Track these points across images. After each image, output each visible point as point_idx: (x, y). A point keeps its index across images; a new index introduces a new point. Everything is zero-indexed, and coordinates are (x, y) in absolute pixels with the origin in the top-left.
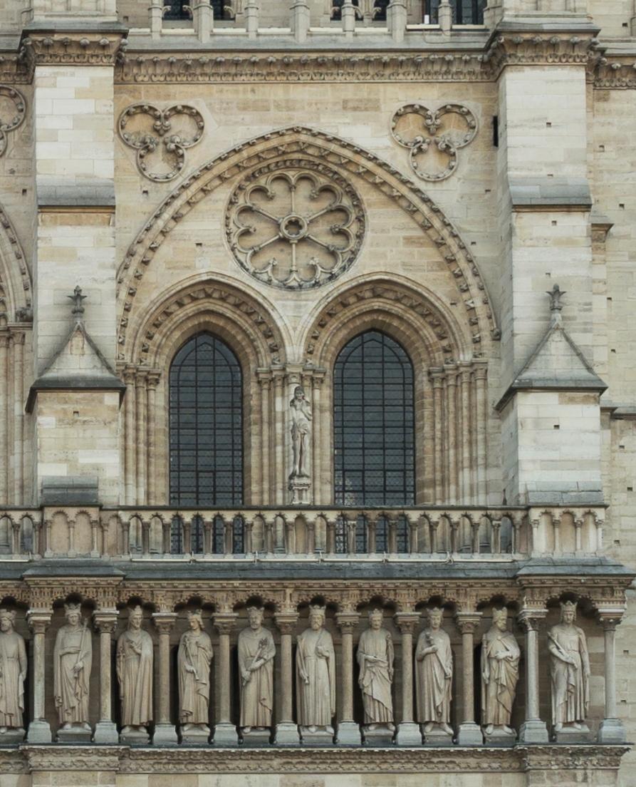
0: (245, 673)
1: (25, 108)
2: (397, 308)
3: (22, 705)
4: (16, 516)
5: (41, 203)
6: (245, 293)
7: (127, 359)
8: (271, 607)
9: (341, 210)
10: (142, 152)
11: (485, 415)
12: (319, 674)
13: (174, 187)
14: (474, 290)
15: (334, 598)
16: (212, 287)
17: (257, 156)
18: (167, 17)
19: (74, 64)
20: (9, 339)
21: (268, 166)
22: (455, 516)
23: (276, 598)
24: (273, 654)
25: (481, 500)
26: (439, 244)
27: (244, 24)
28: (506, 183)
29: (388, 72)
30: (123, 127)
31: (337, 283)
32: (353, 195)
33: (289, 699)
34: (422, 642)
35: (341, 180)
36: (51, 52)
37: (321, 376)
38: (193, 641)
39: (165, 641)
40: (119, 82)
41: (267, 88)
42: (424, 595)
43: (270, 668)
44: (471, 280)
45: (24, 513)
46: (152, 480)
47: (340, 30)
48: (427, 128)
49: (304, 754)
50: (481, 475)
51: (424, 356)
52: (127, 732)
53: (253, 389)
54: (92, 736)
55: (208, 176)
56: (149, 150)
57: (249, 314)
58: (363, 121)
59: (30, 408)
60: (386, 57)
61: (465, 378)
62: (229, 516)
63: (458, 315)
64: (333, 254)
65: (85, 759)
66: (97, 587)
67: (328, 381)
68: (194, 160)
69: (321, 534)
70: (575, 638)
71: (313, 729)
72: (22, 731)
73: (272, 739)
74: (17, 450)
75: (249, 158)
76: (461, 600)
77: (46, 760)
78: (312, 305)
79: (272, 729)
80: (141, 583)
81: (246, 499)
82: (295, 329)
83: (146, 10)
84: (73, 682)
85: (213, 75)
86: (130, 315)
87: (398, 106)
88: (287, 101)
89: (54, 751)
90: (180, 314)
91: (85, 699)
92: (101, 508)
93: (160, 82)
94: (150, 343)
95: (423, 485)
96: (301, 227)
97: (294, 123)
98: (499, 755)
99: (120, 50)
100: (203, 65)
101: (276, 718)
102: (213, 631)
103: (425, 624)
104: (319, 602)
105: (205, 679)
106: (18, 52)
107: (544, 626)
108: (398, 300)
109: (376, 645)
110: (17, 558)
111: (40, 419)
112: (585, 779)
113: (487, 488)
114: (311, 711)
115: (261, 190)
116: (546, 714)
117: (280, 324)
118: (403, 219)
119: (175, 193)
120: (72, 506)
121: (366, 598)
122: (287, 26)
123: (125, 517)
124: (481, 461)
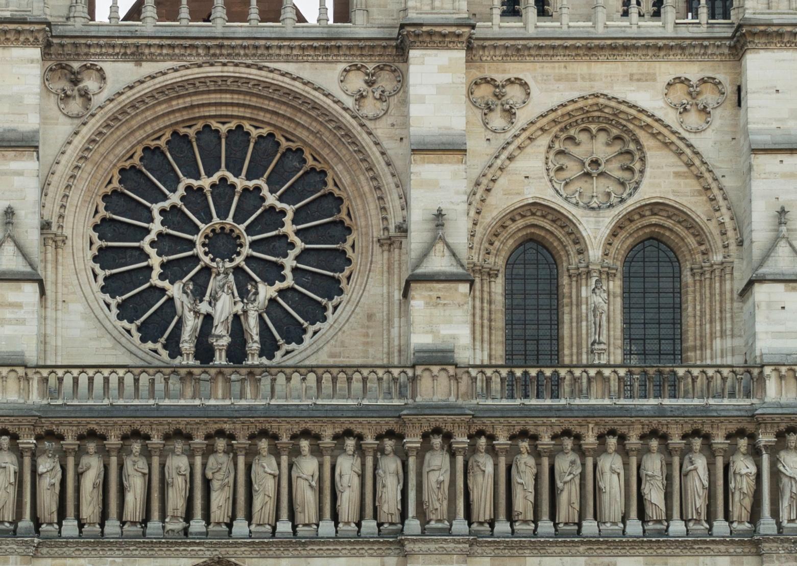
0: (559, 484)
1: (402, 79)
2: (669, 223)
3: (399, 507)
4: (396, 372)
5: (413, 147)
6: (559, 212)
7: (475, 259)
8: (578, 437)
9: (629, 152)
10: (486, 111)
11: (732, 299)
12: (613, 485)
13: (508, 136)
15: (623, 431)
16: (536, 208)
17: (568, 114)
18: (504, 14)
19: (437, 48)
20: (390, 245)
21: (576, 121)
22: (710, 372)
23: (582, 431)
24: (579, 470)
25: (729, 360)
26: (699, 177)
27: (558, 19)
28: (746, 133)
29: (662, 53)
30: (472, 93)
31: (625, 205)
32: (637, 141)
33: (591, 503)
34: (686, 462)
35: (628, 131)
36: (420, 39)
37: (614, 271)
38: (523, 462)
39: (502, 461)
40: (469, 61)
41: (576, 65)
42: (688, 429)
43: (577, 480)
44: (721, 202)
45: (401, 369)
46: (493, 346)
47: (627, 24)
48: (690, 94)
49: (602, 543)
50: (729, 343)
51: (688, 257)
52: (475, 526)
53: (565, 280)
54: (450, 529)
55: (533, 128)
56: (491, 110)
57: (562, 227)
58: (644, 89)
59: (406, 294)
60: (661, 43)
61: (717, 273)
62: (548, 372)
63: (712, 228)
64: (622, 184)
65: (445, 546)
66: (453, 422)
67: (619, 275)
68: (523, 117)
69: (614, 385)
71: (608, 525)
72: (400, 526)
73: (579, 531)
74: (396, 324)
75: (563, 116)
76: (715, 432)
77: (417, 547)
78: (608, 220)
79: (579, 525)
80: (485, 420)
81: (560, 359)
82: (595, 238)
83: (488, 10)
84: (436, 490)
85: (537, 55)
86: (477, 228)
87: (669, 78)
88: (590, 74)
89: (423, 540)
90: (513, 227)
91: (445, 503)
92: (456, 366)
93: (499, 61)
94: (491, 248)
95: (687, 350)
96: (599, 165)
98: (741, 543)
99: (470, 38)
100: (530, 48)
101: (582, 516)
102: (537, 454)
103: (689, 449)
104: (613, 433)
105: (531, 489)
106: (397, 39)
107: (774, 451)
108: (669, 217)
109: (654, 464)
110: (396, 402)
111: (413, 302)
113: (733, 352)
114: (607, 512)
115: (571, 139)
116: (775, 514)
117: (584, 234)
118: (673, 159)
119: (509, 140)
120: (436, 365)
121: (647, 430)
122: (590, 21)
123: (474, 372)
124: (728, 333)
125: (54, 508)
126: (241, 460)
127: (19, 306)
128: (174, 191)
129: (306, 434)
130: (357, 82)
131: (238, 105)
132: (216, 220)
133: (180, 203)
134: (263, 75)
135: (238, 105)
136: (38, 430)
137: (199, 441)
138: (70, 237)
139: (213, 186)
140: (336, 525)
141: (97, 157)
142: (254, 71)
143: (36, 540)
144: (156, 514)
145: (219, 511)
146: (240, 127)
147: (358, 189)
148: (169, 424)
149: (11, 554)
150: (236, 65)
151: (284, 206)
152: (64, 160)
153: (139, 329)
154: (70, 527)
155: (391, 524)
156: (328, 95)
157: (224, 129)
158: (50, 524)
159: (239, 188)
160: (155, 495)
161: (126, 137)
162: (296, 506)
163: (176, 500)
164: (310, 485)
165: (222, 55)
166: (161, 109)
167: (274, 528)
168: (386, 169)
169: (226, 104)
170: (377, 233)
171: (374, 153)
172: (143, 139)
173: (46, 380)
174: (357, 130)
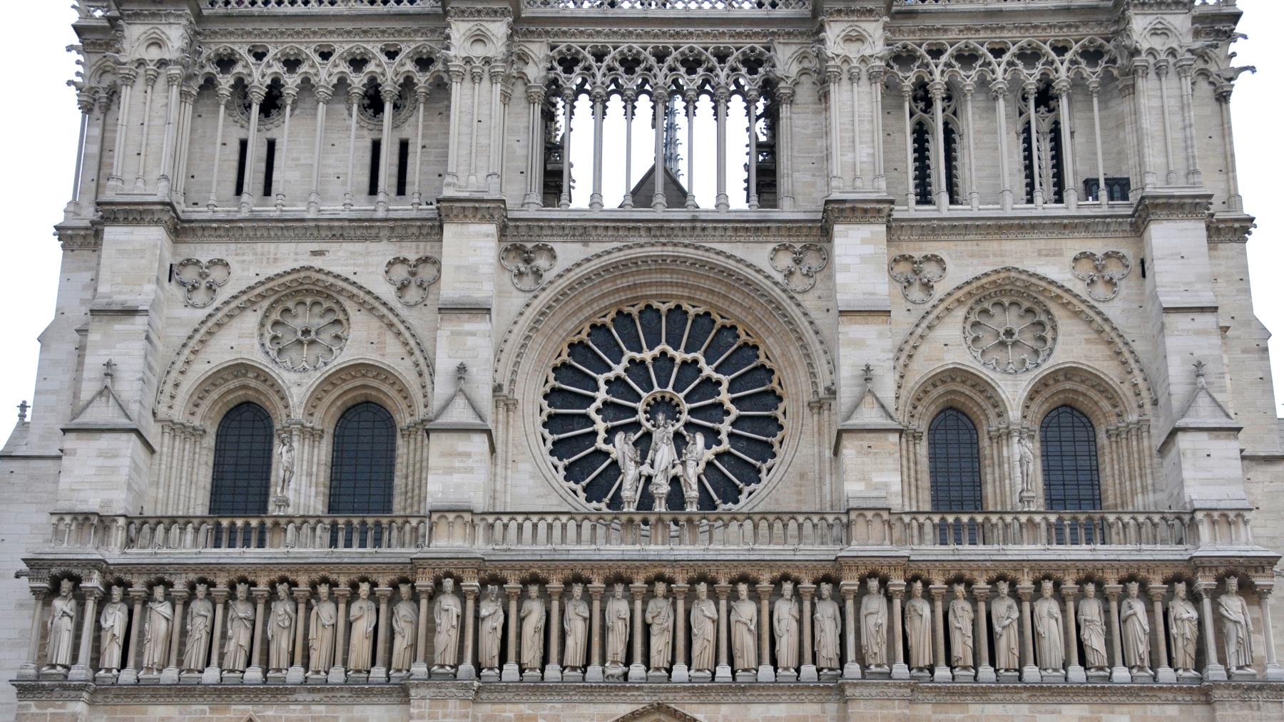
0: (997, 629)
1: (827, 259)
2: (1082, 388)
8: (1013, 584)
9: (1041, 324)
11: (1151, 456)
13: (928, 307)
14: (1136, 372)
16: (956, 374)
17: (983, 287)
18: (918, 203)
20: (820, 407)
23: (1019, 575)
26: (1110, 343)
31: (1040, 370)
32: (1048, 312)
35: (1039, 303)
43: (1015, 625)
48: (1096, 267)
49: (1045, 689)
50: (1151, 497)
55: (951, 299)
57: (982, 392)
58: (1054, 263)
59: (836, 452)
61: (1134, 432)
63: (1126, 390)
64: (1036, 352)
68: (940, 290)
70: (1239, 603)
73: (1020, 678)
75: (977, 288)
77: (857, 692)
79: (1020, 670)
87: (1076, 253)
90: (935, 393)
97: (1007, 265)
98: (1190, 691)
101: (1022, 662)
102: (972, 599)
103: (1125, 594)
108: (1083, 382)
109: (1092, 609)
121: (1082, 575)
123: (907, 519)
124: (1150, 488)
125: (496, 652)
126: (681, 605)
127: (468, 455)
128: (618, 362)
129: (744, 579)
130: (785, 260)
131: (677, 285)
132: (657, 389)
133: (623, 374)
134: (699, 255)
135: (677, 285)
137: (639, 584)
138: (520, 401)
139: (654, 359)
140: (776, 670)
141: (548, 331)
142: (691, 251)
143: (476, 684)
146: (678, 307)
147: (788, 360)
148: (610, 568)
150: (675, 245)
151: (720, 376)
152: (516, 329)
153: (585, 490)
154: (511, 670)
155: (830, 669)
156: (759, 271)
157: (664, 308)
158: (491, 669)
159: (678, 361)
161: (574, 313)
162: (735, 651)
163: (616, 645)
164: (749, 630)
165: (662, 236)
166: (607, 287)
167: (714, 674)
168: (814, 337)
169: (666, 284)
170: (807, 396)
171: (803, 323)
172: (590, 316)
173: (492, 526)
174: (787, 303)
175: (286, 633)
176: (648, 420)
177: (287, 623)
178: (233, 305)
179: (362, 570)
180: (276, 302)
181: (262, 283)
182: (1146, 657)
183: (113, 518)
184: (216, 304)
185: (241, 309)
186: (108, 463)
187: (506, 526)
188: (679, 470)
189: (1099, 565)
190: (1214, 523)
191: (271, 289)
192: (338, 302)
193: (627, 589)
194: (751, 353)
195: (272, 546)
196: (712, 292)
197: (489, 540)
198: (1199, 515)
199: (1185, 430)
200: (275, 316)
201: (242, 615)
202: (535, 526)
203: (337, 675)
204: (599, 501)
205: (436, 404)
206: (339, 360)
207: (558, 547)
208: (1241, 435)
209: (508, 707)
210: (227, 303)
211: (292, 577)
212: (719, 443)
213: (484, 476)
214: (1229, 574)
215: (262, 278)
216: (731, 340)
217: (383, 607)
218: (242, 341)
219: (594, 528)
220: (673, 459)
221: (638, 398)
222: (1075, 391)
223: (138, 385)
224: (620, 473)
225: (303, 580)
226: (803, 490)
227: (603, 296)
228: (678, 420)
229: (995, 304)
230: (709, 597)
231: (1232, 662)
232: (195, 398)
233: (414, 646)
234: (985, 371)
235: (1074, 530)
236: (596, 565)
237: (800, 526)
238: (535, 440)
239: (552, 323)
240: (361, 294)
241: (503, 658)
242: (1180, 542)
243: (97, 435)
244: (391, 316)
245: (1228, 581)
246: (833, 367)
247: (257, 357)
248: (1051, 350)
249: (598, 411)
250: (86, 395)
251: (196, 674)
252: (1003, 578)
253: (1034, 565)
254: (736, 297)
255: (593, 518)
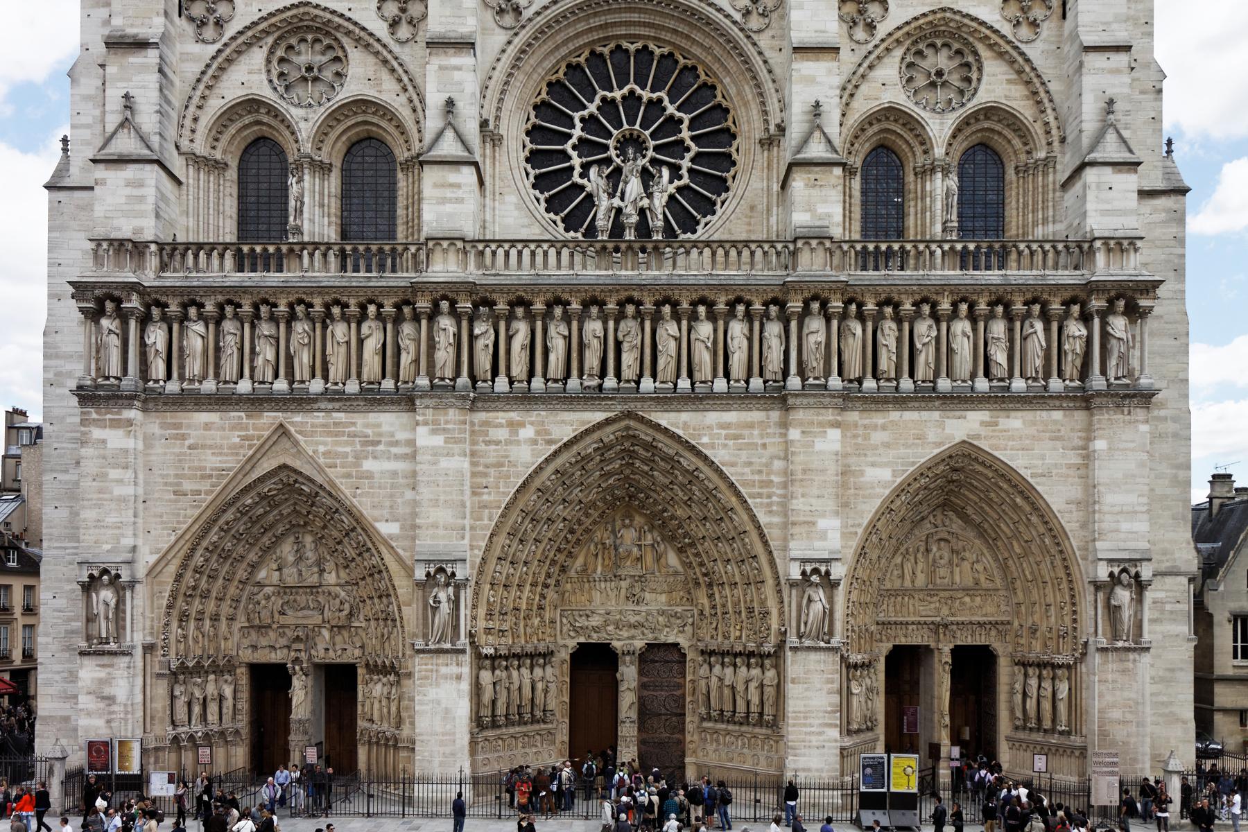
0: (919, 346)
8: (934, 305)
9: (968, 65)
12: (963, 348)
16: (891, 113)
20: (770, 144)
26: (1028, 83)
32: (975, 53)
33: (945, 363)
35: (968, 44)
39: (870, 325)
44: (1047, 104)
48: (1022, 9)
57: (911, 130)
59: (784, 185)
63: (1038, 129)
64: (961, 92)
77: (798, 401)
90: (870, 131)
101: (937, 374)
102: (898, 320)
108: (999, 121)
112: (1129, 413)
115: (919, 53)
116: (1104, 372)
125: (488, 367)
126: (648, 325)
128: (591, 101)
129: (703, 301)
131: (645, 25)
132: (626, 126)
135: (645, 25)
136: (474, 297)
137: (611, 306)
139: (624, 97)
143: (472, 395)
144: (575, 372)
145: (629, 372)
146: (645, 47)
147: (743, 99)
148: (586, 291)
149: (451, 407)
154: (502, 384)
155: (775, 381)
157: (632, 48)
158: (485, 381)
159: (645, 100)
160: (574, 355)
163: (592, 360)
164: (707, 347)
166: (581, 27)
167: (676, 385)
170: (759, 134)
173: (482, 253)
175: (306, 349)
176: (618, 156)
177: (306, 341)
178: (240, 41)
179: (369, 293)
180: (280, 38)
181: (264, 19)
182: (1040, 370)
183: (146, 244)
184: (225, 39)
185: (249, 45)
186: (136, 192)
187: (494, 253)
188: (645, 203)
189: (1008, 289)
190: (1109, 250)
191: (274, 25)
192: (336, 39)
193: (601, 310)
194: (709, 93)
195: (289, 271)
196: (675, 31)
197: (481, 265)
198: (1098, 244)
199: (1093, 164)
200: (280, 53)
201: (266, 333)
202: (520, 253)
203: (352, 387)
204: (576, 231)
205: (428, 137)
206: (341, 96)
207: (541, 272)
208: (1140, 168)
209: (501, 414)
210: (233, 38)
211: (308, 299)
212: (680, 178)
213: (475, 208)
214: (1118, 297)
215: (264, 14)
216: (691, 80)
217: (389, 327)
218: (250, 77)
219: (572, 255)
220: (641, 194)
221: (609, 135)
222: (992, 130)
223: (156, 117)
224: (594, 205)
225: (317, 302)
226: (753, 221)
227: (578, 35)
228: (644, 156)
229: (928, 46)
230: (672, 317)
231: (1112, 373)
232: (214, 132)
233: (417, 361)
234: (916, 109)
235: (988, 255)
236: (574, 288)
237: (752, 253)
238: (519, 174)
239: (532, 61)
240: (357, 31)
241: (495, 372)
242: (1076, 268)
243: (124, 166)
244: (385, 53)
245: (1117, 303)
246: (784, 106)
247: (267, 93)
248: (976, 90)
249: (574, 147)
250: (110, 128)
251: (232, 385)
252: (926, 300)
253: (952, 289)
254: (697, 36)
255: (571, 245)
